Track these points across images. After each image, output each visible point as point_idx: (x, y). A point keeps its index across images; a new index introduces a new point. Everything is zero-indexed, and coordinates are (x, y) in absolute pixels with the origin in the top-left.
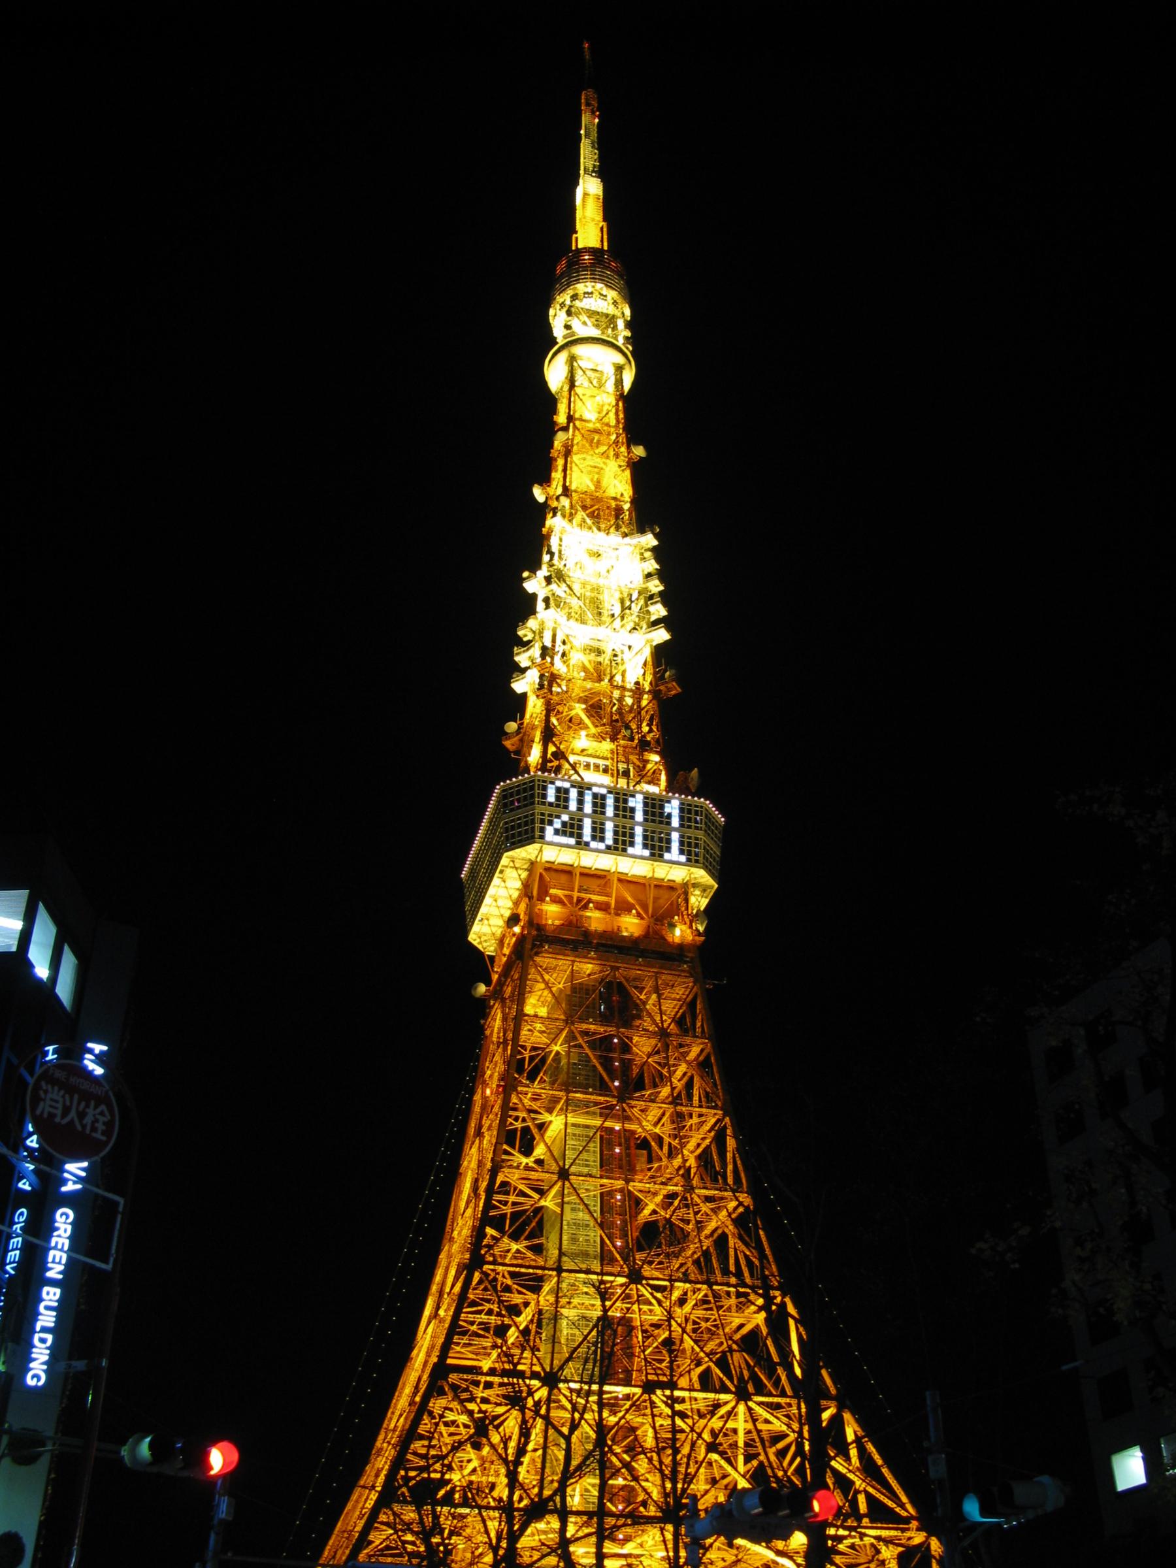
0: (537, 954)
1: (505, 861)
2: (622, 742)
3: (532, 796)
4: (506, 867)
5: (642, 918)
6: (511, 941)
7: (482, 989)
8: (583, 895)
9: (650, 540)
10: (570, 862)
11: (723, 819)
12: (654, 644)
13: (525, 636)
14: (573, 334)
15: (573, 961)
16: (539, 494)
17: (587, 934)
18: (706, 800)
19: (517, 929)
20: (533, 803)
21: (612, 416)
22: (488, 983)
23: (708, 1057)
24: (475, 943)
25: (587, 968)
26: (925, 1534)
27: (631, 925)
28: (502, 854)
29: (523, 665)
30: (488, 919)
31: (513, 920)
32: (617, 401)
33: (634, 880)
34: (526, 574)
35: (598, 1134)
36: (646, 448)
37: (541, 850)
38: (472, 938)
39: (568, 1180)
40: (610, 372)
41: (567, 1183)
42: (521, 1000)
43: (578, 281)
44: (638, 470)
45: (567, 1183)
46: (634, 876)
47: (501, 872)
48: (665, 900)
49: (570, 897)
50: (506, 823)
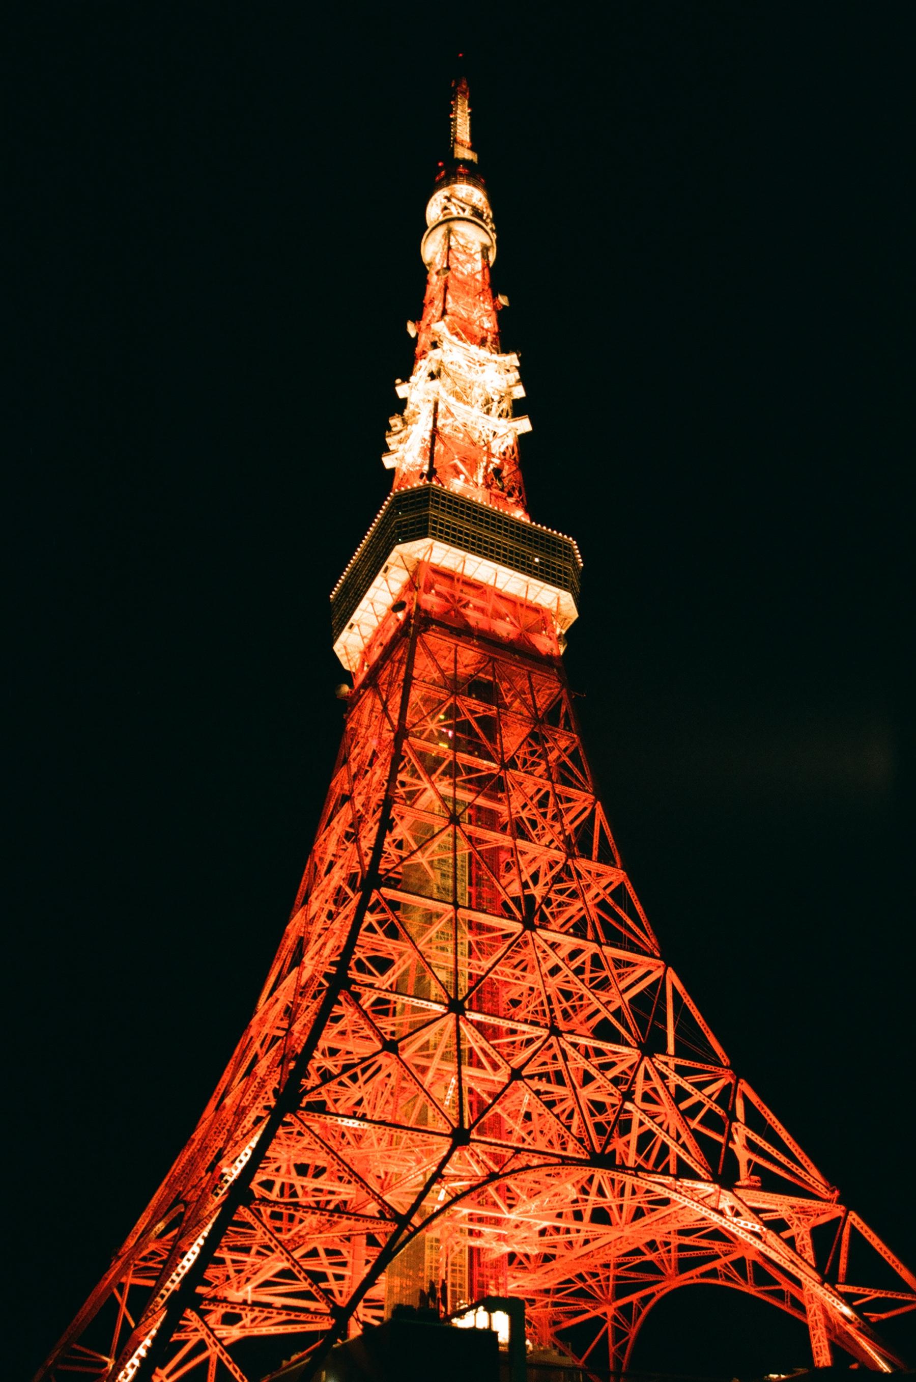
0: (425, 631)
2: (495, 491)
3: (427, 501)
4: (393, 564)
5: (515, 626)
6: (393, 627)
7: (346, 689)
8: (463, 595)
9: (513, 359)
10: (453, 567)
11: (582, 565)
12: (519, 433)
13: (396, 426)
14: (451, 213)
15: (457, 645)
16: (411, 329)
17: (467, 624)
18: (574, 540)
19: (401, 615)
20: (428, 506)
21: (479, 277)
22: (351, 685)
23: (576, 750)
24: (338, 654)
25: (469, 656)
26: (843, 1208)
27: (504, 629)
29: (391, 448)
30: (359, 626)
31: (398, 606)
32: (483, 269)
33: (507, 597)
34: (398, 381)
35: (467, 812)
36: (510, 301)
37: (431, 548)
38: (338, 648)
39: (459, 825)
40: (477, 248)
41: (458, 828)
42: (410, 665)
43: (455, 182)
44: (502, 315)
45: (458, 828)
46: (507, 593)
47: (386, 571)
48: (532, 618)
49: (453, 596)
50: (397, 522)
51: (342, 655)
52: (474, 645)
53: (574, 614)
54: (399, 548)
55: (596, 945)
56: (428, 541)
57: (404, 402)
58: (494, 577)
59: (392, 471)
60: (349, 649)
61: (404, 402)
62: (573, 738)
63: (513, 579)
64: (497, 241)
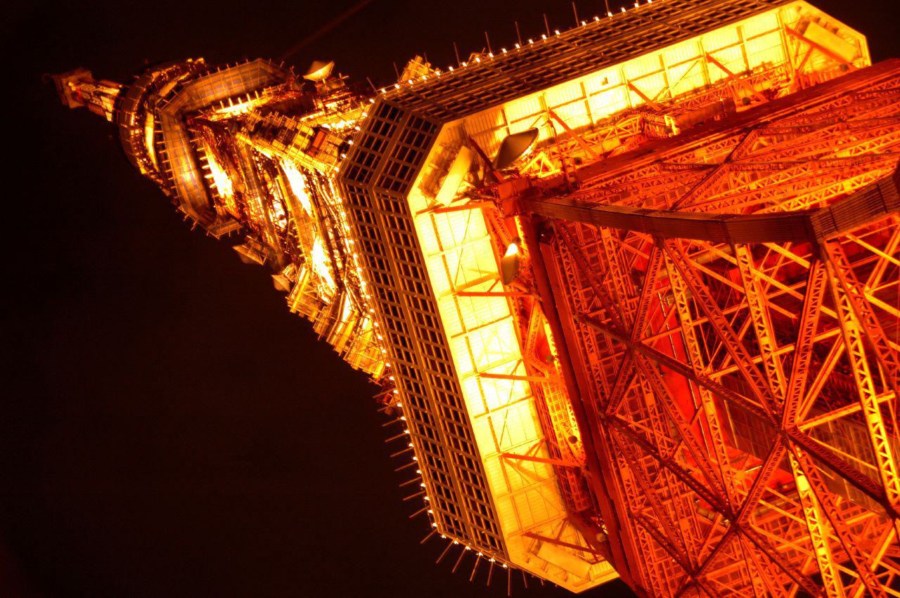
1: (423, 226)
28: (406, 211)
38: (518, 555)
54: (416, 199)
60: (547, 533)
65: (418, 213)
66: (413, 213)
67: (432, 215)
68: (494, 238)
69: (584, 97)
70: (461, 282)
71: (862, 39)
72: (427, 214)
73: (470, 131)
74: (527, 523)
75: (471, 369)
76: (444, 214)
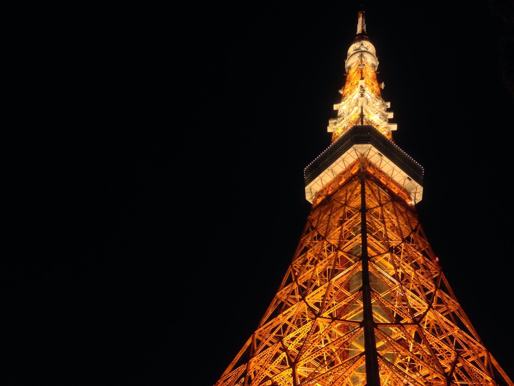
1: (351, 149)
24: (306, 191)
38: (307, 188)
51: (307, 192)
52: (386, 191)
53: (419, 198)
54: (355, 146)
55: (459, 328)
56: (370, 146)
57: (337, 111)
58: (392, 171)
59: (331, 134)
60: (312, 190)
61: (337, 111)
62: (426, 244)
63: (399, 175)
64: (378, 65)
65: (353, 147)
66: (353, 147)
67: (353, 150)
68: (356, 161)
69: (388, 163)
70: (345, 159)
71: (421, 199)
72: (353, 149)
73: (372, 149)
74: (312, 187)
75: (332, 167)
76: (355, 151)
